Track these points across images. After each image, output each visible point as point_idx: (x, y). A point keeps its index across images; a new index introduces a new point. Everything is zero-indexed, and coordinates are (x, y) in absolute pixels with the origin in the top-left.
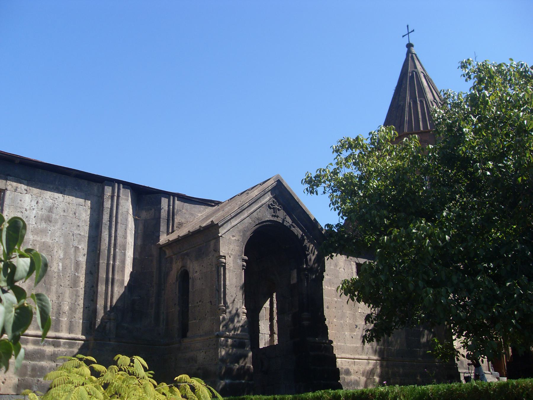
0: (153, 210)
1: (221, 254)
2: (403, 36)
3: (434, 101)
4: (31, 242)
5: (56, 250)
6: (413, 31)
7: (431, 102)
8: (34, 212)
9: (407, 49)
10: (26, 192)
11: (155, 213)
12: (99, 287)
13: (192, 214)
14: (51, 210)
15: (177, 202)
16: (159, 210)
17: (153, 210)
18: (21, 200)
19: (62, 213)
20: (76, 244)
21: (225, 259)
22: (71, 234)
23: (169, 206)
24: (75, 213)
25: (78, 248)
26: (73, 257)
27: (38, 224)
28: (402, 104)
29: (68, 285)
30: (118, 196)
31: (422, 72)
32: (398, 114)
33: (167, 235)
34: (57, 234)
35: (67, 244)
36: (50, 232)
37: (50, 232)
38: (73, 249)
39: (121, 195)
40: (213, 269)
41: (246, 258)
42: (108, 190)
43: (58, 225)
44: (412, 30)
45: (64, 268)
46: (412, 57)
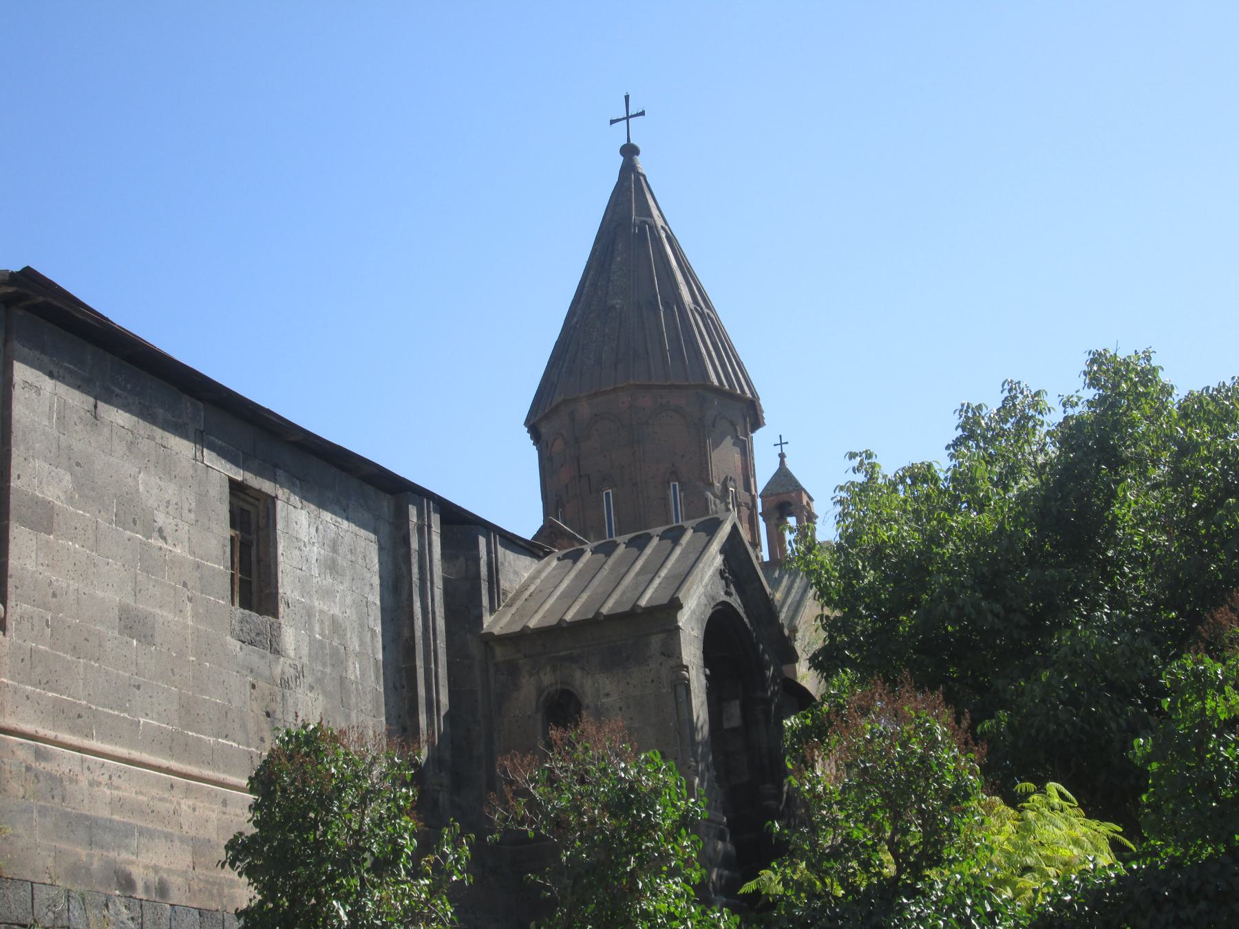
0: (462, 559)
1: (685, 663)
2: (612, 122)
3: (697, 311)
4: (317, 615)
5: (349, 635)
6: (643, 113)
7: (691, 310)
8: (315, 548)
9: (621, 159)
10: (299, 505)
11: (467, 566)
12: (420, 717)
13: (516, 573)
14: (334, 549)
15: (499, 547)
16: (478, 559)
17: (462, 559)
18: (296, 523)
19: (349, 556)
20: (372, 624)
21: (688, 671)
22: (365, 600)
23: (489, 553)
24: (365, 557)
25: (375, 631)
26: (370, 652)
27: (323, 576)
28: (618, 306)
29: (371, 711)
30: (430, 527)
31: (662, 227)
32: (607, 330)
33: (491, 614)
34: (349, 600)
35: (361, 626)
36: (338, 594)
37: (338, 594)
38: (369, 635)
39: (433, 525)
40: (664, 691)
41: (708, 672)
42: (413, 511)
43: (347, 584)
44: (640, 111)
45: (363, 674)
46: (638, 181)
